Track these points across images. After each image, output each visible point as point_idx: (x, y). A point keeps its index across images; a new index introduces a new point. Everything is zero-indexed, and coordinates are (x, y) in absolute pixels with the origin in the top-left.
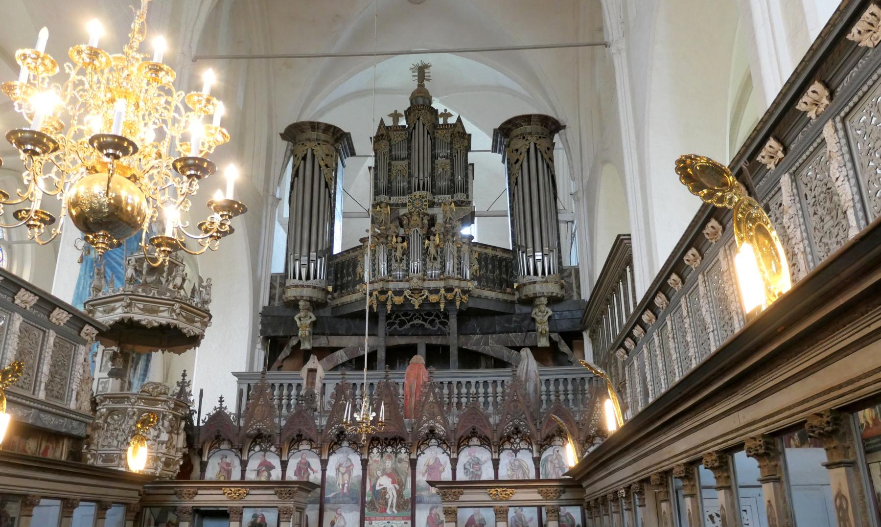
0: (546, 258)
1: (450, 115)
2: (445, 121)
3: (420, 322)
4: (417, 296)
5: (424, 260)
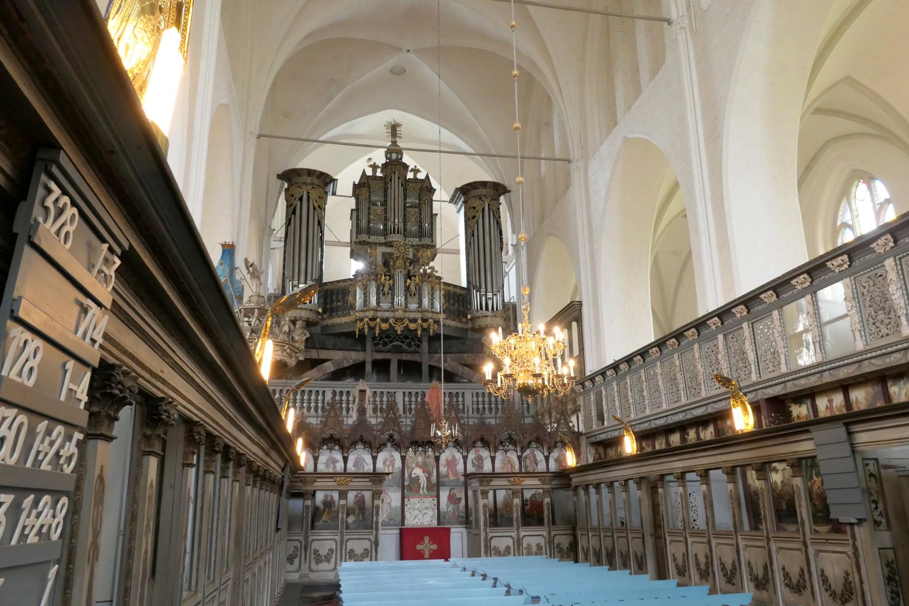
1: (419, 171)
2: (415, 175)
4: (399, 323)
5: (406, 295)
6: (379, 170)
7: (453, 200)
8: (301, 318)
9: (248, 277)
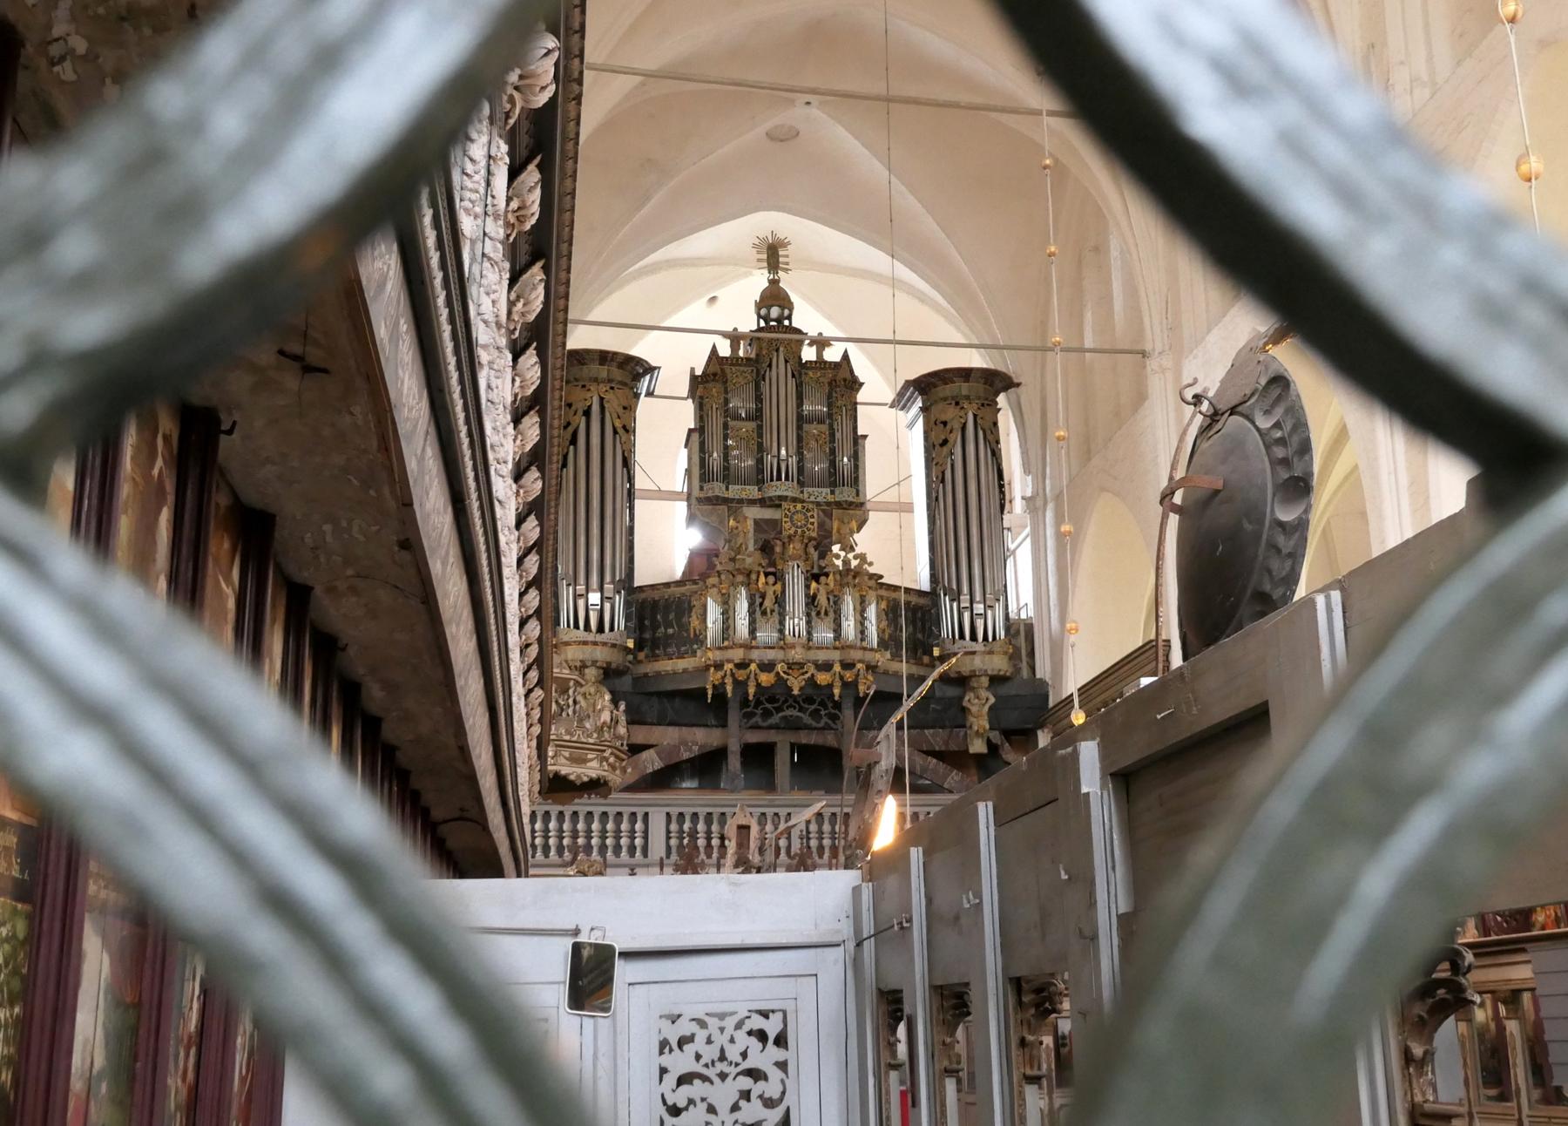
0: (989, 613)
2: (819, 354)
3: (796, 713)
4: (796, 674)
5: (808, 615)
7: (901, 402)
8: (594, 663)
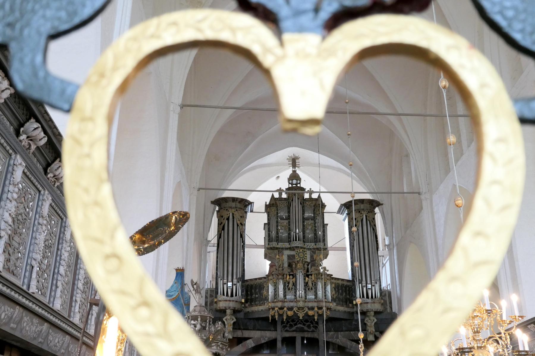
0: (373, 288)
2: (310, 195)
4: (301, 311)
5: (305, 290)
6: (283, 193)
7: (340, 212)
8: (229, 308)
9: (194, 292)
